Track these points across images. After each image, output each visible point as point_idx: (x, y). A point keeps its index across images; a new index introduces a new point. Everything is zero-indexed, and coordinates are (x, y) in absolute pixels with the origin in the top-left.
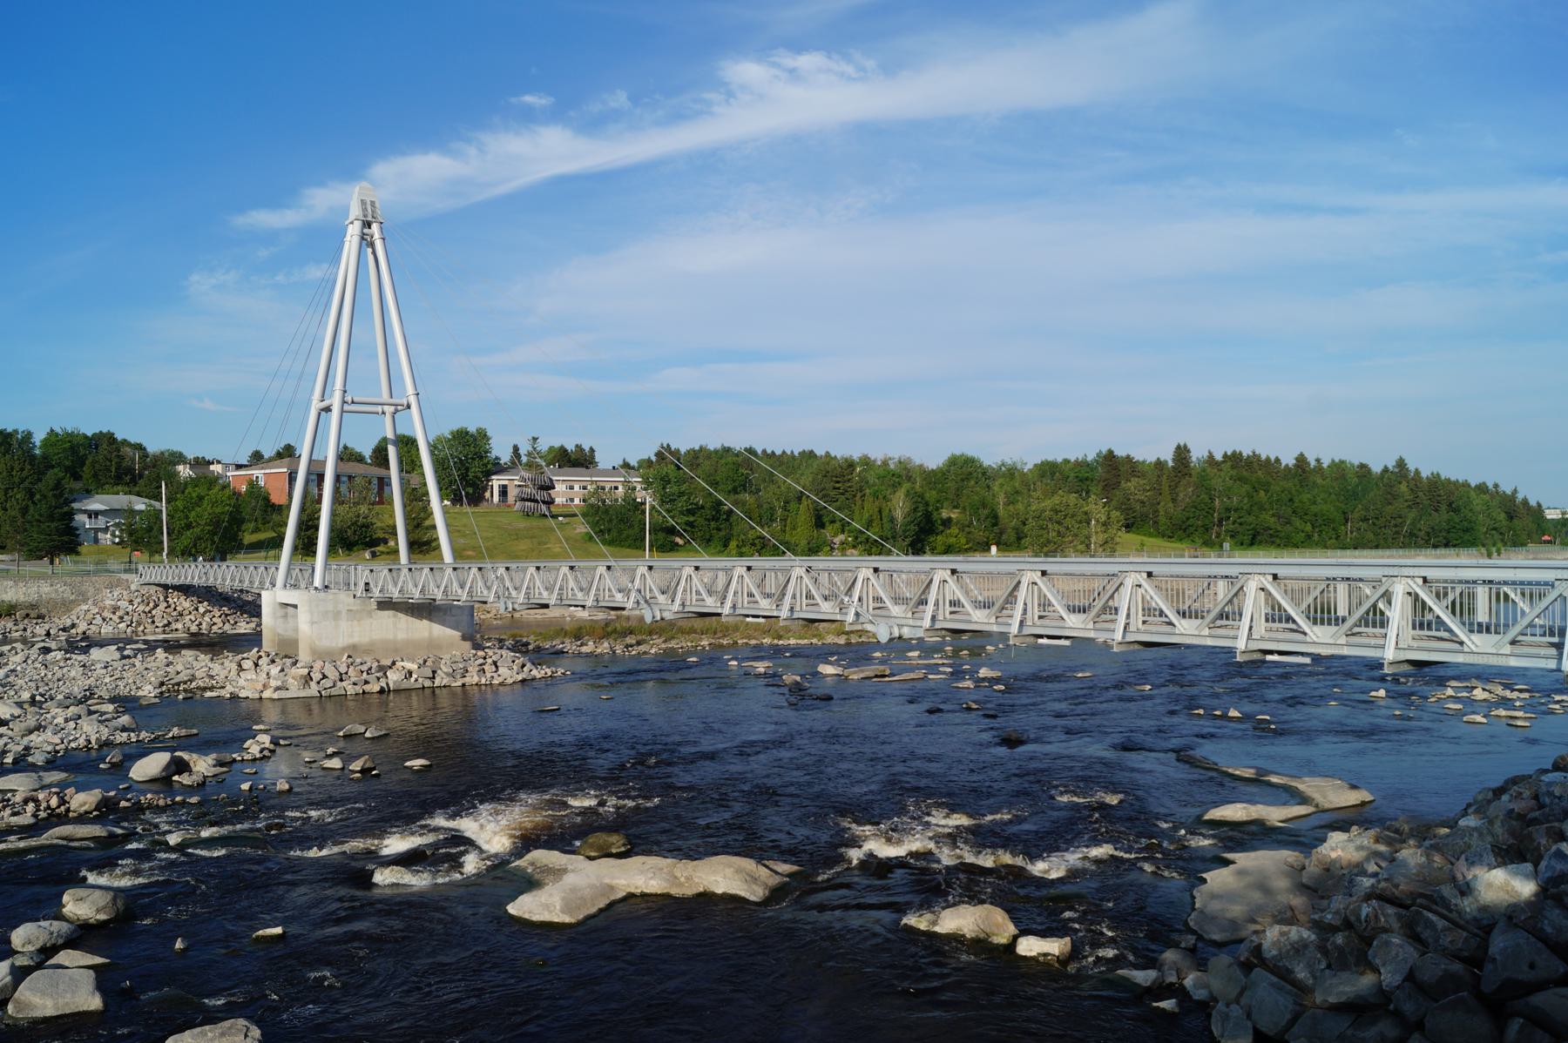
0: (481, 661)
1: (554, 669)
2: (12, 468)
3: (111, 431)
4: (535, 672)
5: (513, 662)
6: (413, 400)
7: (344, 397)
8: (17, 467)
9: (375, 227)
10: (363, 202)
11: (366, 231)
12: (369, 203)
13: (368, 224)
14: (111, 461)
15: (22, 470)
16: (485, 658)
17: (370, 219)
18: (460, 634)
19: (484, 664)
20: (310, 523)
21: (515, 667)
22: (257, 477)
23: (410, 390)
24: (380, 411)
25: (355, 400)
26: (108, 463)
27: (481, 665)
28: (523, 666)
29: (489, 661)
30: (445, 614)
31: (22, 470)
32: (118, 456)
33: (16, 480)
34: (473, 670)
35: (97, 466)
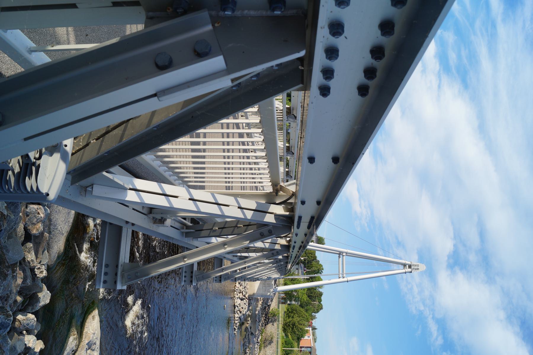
0: (244, 293)
1: (237, 326)
2: (312, 254)
3: (323, 309)
4: (236, 315)
5: (242, 308)
6: (345, 279)
7: (345, 253)
8: (312, 255)
9: (410, 270)
10: (418, 266)
11: (407, 266)
12: (418, 268)
13: (410, 267)
14: (314, 294)
15: (311, 257)
16: (245, 296)
17: (412, 267)
18: (255, 292)
19: (243, 295)
20: (295, 327)
21: (240, 307)
22: (309, 337)
23: (350, 278)
24: (340, 276)
25: (344, 257)
26: (313, 293)
27: (242, 293)
28: (240, 312)
29: (244, 297)
30: (263, 284)
31: (311, 257)
32: (315, 297)
33: (308, 255)
34: (241, 295)
35: (312, 290)
